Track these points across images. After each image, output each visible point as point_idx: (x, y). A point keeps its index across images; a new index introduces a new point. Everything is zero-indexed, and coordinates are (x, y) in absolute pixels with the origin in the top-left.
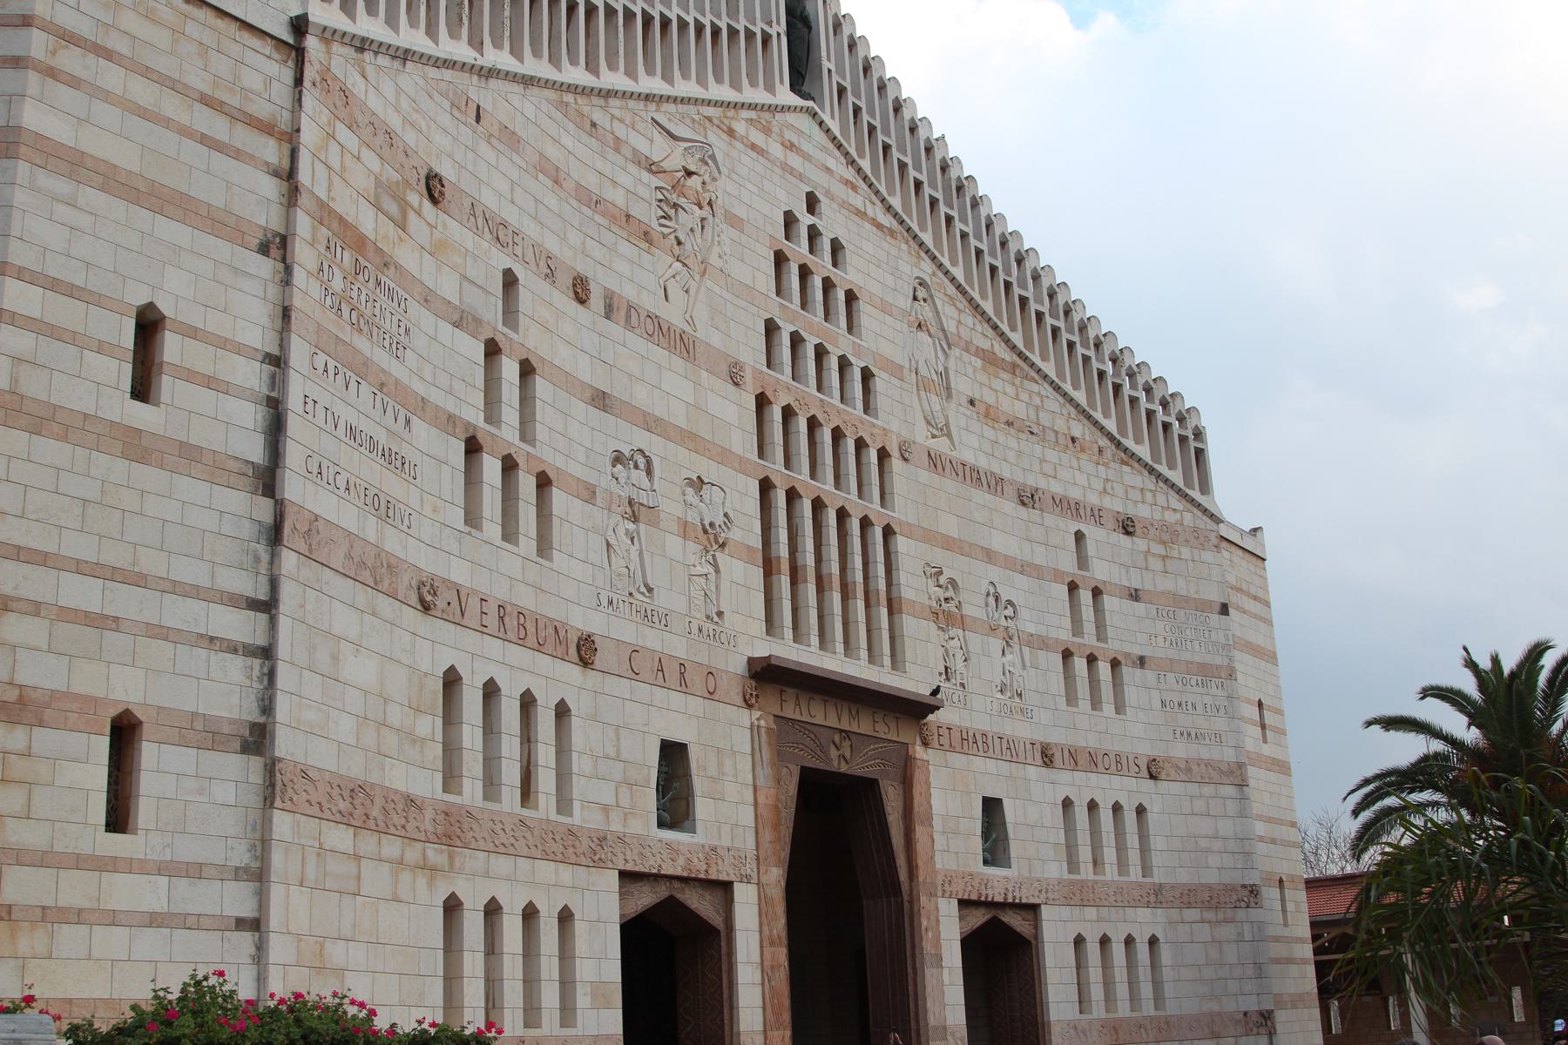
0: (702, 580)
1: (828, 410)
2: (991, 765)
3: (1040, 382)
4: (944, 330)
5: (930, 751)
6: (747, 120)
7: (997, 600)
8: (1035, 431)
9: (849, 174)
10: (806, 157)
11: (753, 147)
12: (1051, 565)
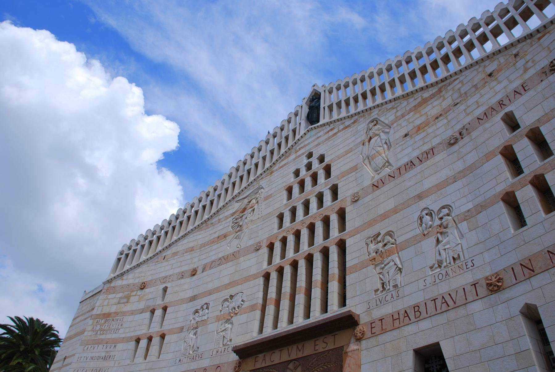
0: (224, 333)
1: (304, 221)
2: (424, 325)
3: (459, 77)
4: (387, 125)
5: (364, 342)
6: (280, 162)
7: (431, 215)
8: (458, 101)
9: (332, 126)
10: (309, 144)
11: (281, 167)
12: (482, 155)
